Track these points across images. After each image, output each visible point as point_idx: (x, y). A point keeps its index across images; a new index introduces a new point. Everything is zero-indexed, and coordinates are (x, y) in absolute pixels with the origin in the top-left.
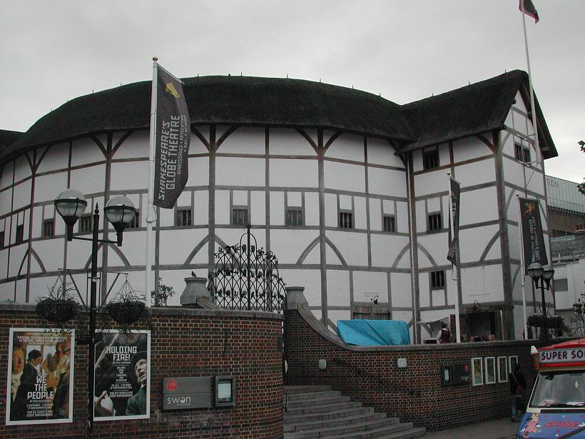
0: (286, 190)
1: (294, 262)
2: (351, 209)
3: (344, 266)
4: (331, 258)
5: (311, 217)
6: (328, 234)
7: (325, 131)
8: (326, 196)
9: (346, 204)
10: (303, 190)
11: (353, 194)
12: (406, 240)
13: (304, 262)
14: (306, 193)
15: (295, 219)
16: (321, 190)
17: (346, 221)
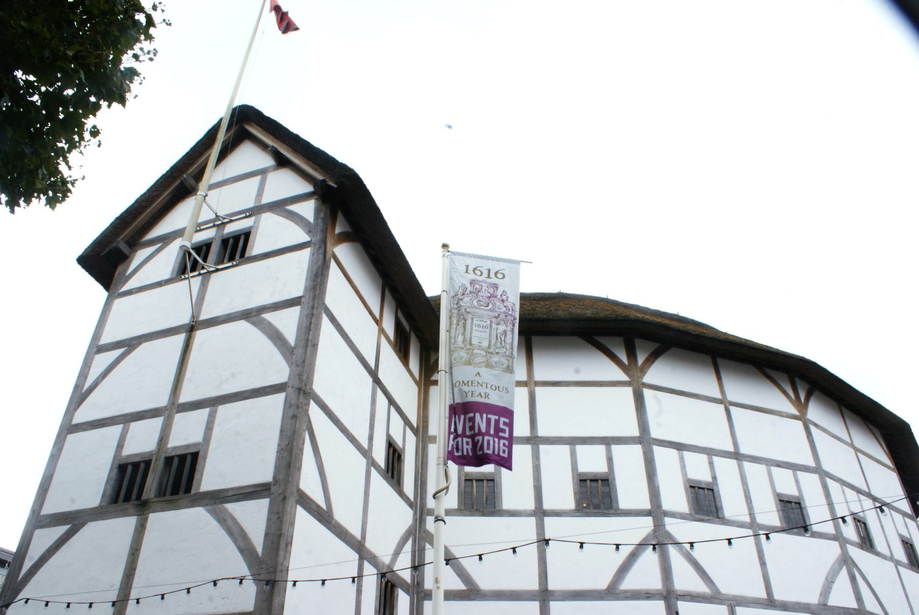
0: (573, 442)
1: (602, 584)
2: (709, 479)
3: (715, 598)
4: (685, 579)
5: (630, 491)
6: (671, 525)
7: (638, 342)
8: (658, 451)
9: (699, 469)
10: (608, 441)
11: (710, 452)
12: (833, 549)
13: (628, 584)
14: (615, 448)
15: (596, 495)
16: (645, 439)
17: (705, 501)
